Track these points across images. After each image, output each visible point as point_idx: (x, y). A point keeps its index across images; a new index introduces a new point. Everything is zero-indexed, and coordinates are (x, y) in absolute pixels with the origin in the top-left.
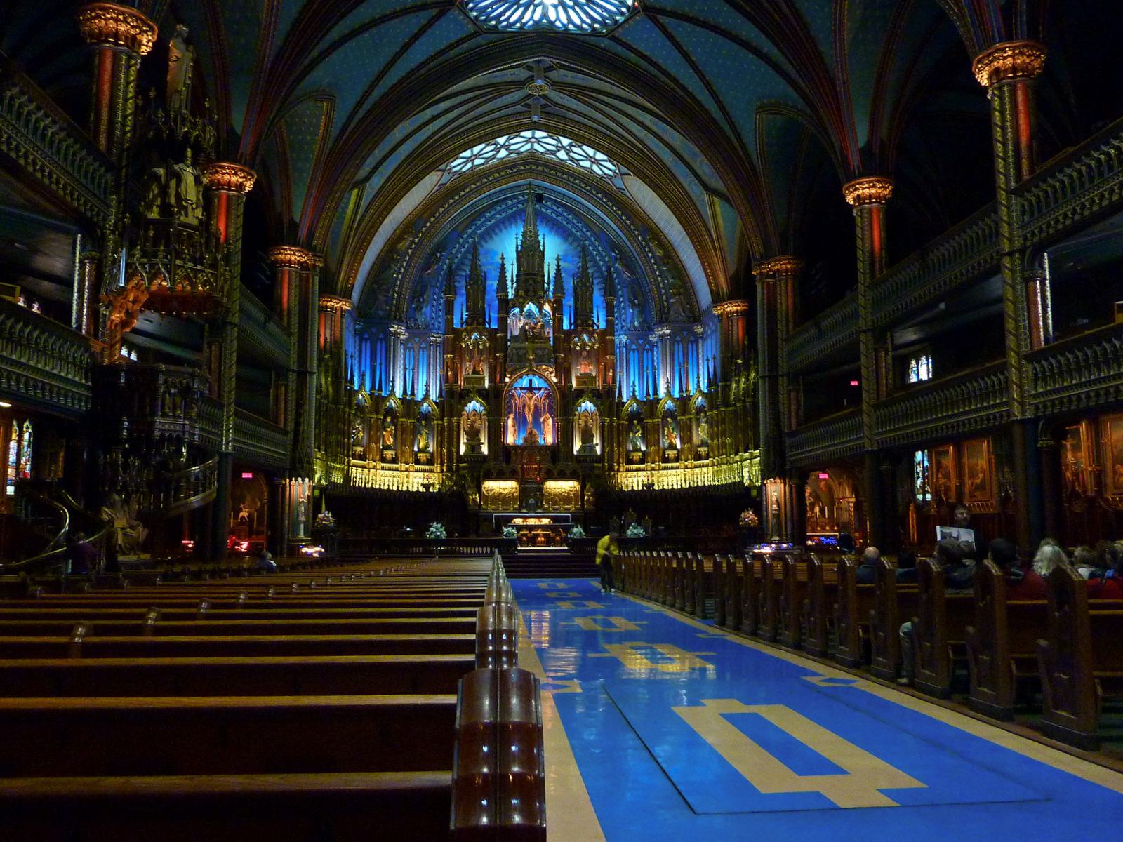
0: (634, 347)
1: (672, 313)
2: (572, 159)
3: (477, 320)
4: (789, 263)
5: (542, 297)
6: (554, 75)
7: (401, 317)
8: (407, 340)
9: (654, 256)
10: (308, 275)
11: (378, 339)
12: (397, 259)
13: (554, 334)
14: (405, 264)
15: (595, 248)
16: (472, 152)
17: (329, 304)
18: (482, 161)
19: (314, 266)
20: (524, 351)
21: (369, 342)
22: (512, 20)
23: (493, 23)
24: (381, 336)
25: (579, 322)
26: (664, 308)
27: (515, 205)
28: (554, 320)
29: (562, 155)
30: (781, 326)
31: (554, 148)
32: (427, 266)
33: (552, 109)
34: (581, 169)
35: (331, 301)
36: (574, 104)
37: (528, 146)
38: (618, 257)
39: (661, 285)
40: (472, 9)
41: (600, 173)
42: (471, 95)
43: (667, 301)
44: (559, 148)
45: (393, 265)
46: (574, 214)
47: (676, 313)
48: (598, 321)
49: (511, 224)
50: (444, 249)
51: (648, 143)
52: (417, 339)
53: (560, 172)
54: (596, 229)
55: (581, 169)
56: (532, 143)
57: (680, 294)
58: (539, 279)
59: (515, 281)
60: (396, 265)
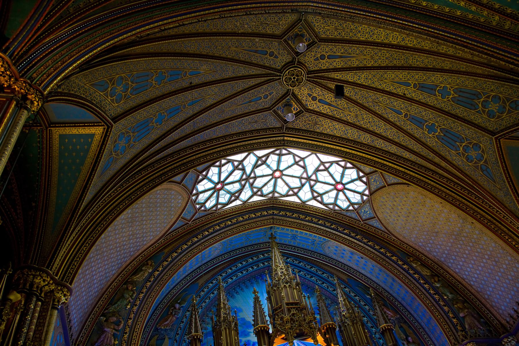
1: (467, 327)
2: (317, 196)
14: (142, 295)
26: (455, 326)
27: (256, 263)
29: (305, 194)
31: (295, 183)
32: (165, 317)
39: (442, 303)
43: (456, 316)
45: (127, 296)
46: (318, 266)
49: (252, 283)
50: (184, 300)
53: (303, 214)
54: (344, 278)
56: (276, 178)
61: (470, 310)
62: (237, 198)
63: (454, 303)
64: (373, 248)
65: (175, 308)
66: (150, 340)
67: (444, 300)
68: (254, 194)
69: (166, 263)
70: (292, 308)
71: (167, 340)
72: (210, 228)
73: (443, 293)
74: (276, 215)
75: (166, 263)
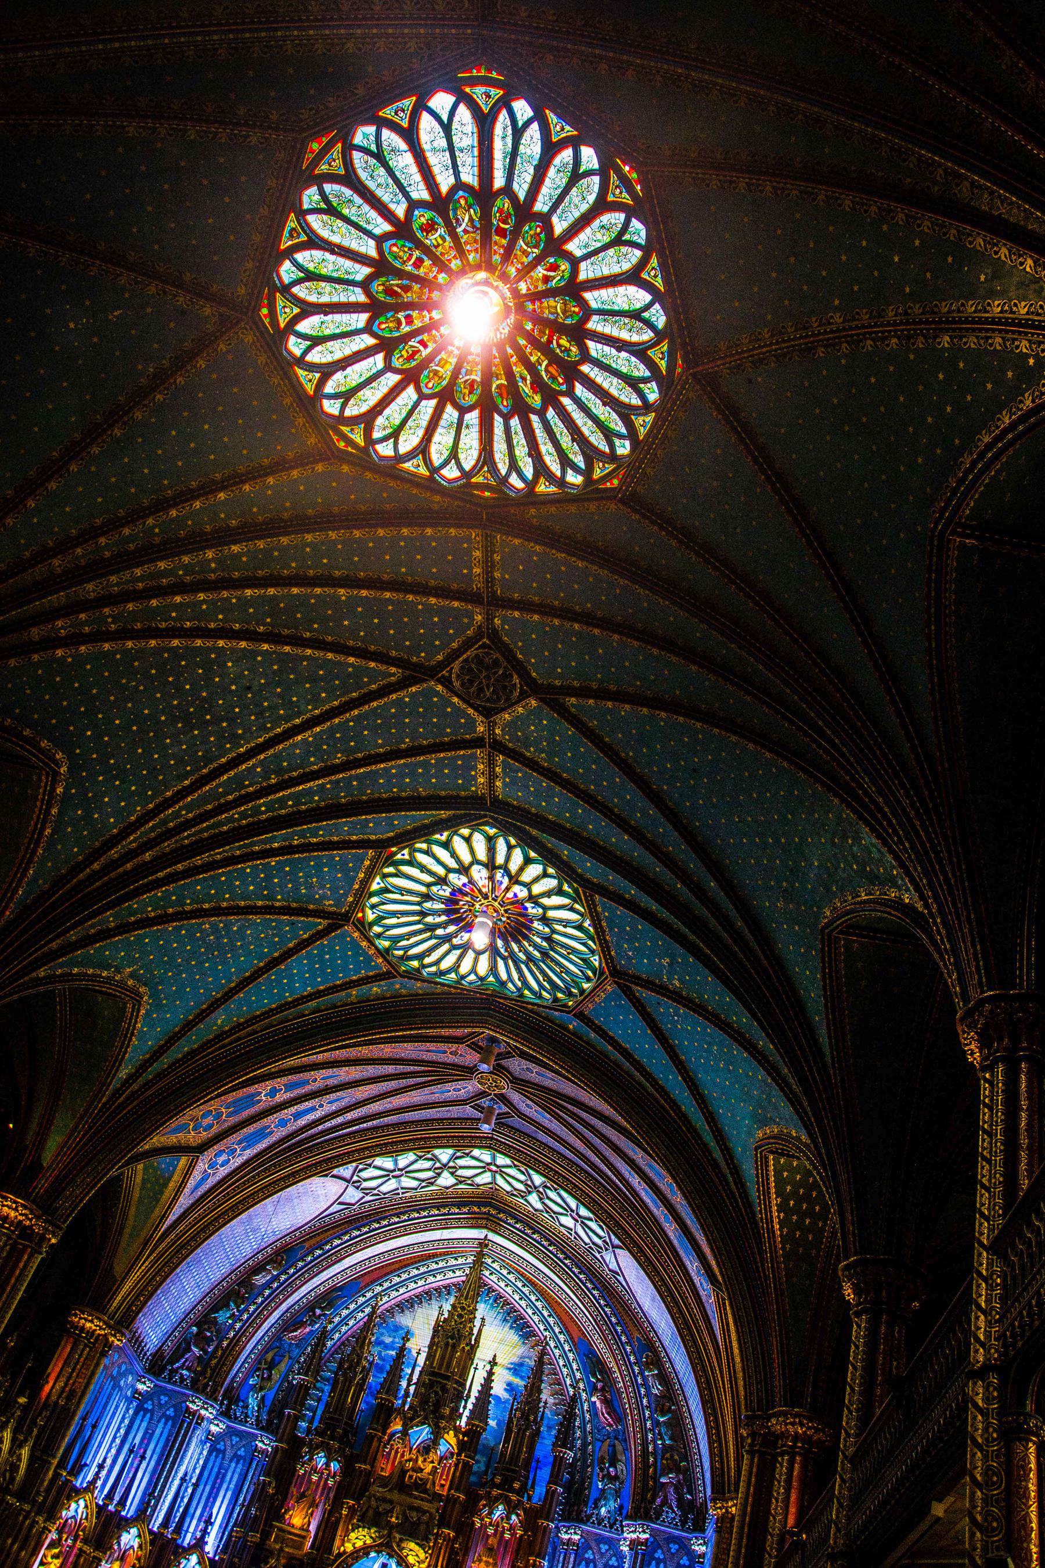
0: (589, 1555)
1: (658, 1500)
3: (333, 1431)
4: (802, 1425)
5: (443, 1417)
6: (516, 1065)
7: (215, 1391)
8: (219, 1437)
9: (648, 1394)
10: (26, 1247)
11: (164, 1415)
12: (243, 1297)
13: (450, 1489)
14: (252, 1308)
15: (568, 1364)
16: (396, 1162)
17: (88, 1325)
18: (414, 1184)
19: (43, 1238)
20: (388, 1507)
21: (148, 1415)
22: (445, 965)
23: (415, 964)
24: (170, 1412)
25: (498, 1480)
28: (456, 1465)
30: (771, 1543)
33: (515, 1121)
34: (562, 1229)
35: (92, 1321)
36: (546, 1119)
37: (486, 1178)
38: (599, 1385)
40: (379, 936)
41: (587, 1240)
42: (390, 1069)
44: (531, 1188)
47: (661, 1506)
48: (533, 1486)
50: (330, 1305)
51: (643, 1194)
52: (235, 1439)
54: (575, 1334)
55: (562, 1229)
57: (678, 1470)
58: (449, 1385)
59: (415, 1380)
60: (238, 1307)
61: (681, 1477)
62: (432, 1184)
63: (668, 1455)
64: (608, 1318)
65: (314, 1313)
66: (266, 1352)
67: (655, 1446)
68: (461, 1182)
69: (301, 1264)
70: (437, 1382)
71: (286, 1359)
72: (384, 1219)
73: (660, 1434)
74: (492, 1215)
75: (301, 1264)
